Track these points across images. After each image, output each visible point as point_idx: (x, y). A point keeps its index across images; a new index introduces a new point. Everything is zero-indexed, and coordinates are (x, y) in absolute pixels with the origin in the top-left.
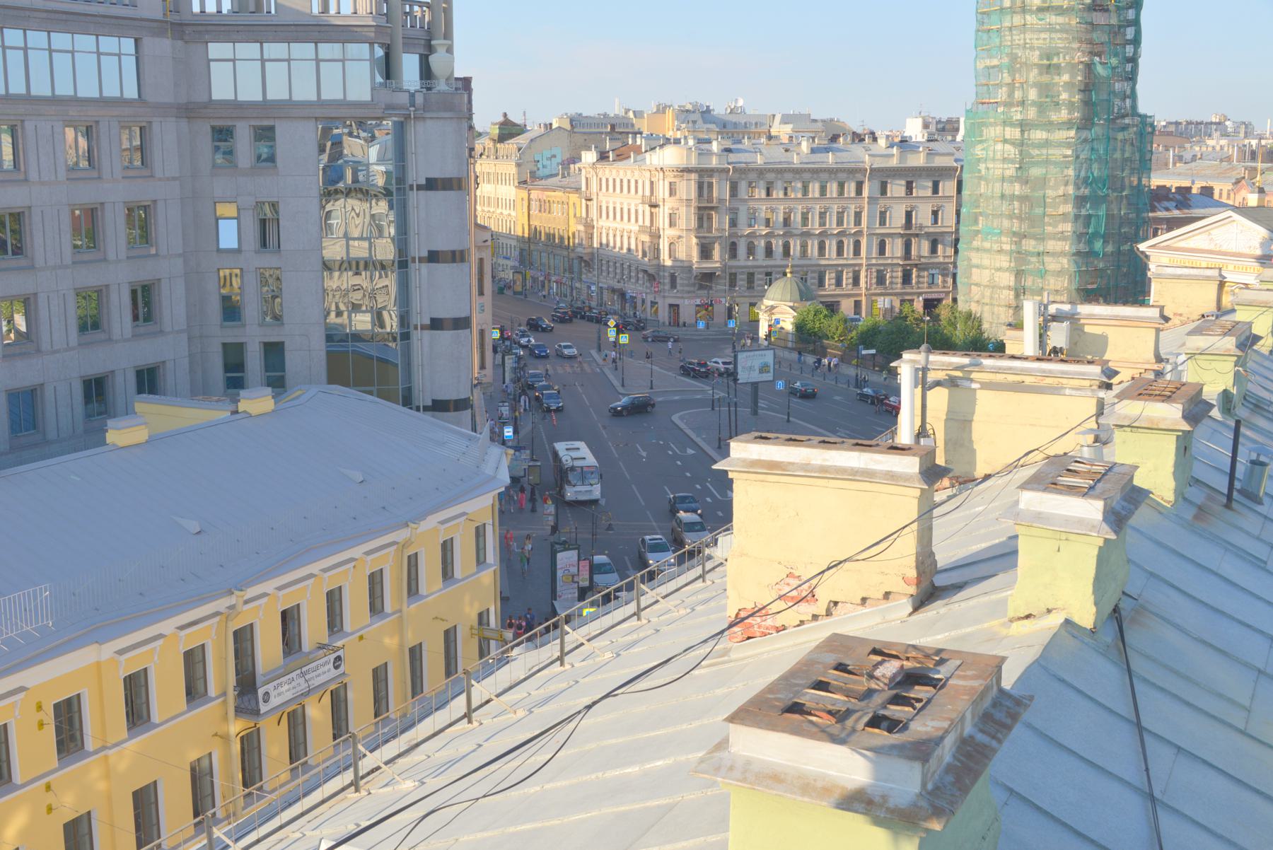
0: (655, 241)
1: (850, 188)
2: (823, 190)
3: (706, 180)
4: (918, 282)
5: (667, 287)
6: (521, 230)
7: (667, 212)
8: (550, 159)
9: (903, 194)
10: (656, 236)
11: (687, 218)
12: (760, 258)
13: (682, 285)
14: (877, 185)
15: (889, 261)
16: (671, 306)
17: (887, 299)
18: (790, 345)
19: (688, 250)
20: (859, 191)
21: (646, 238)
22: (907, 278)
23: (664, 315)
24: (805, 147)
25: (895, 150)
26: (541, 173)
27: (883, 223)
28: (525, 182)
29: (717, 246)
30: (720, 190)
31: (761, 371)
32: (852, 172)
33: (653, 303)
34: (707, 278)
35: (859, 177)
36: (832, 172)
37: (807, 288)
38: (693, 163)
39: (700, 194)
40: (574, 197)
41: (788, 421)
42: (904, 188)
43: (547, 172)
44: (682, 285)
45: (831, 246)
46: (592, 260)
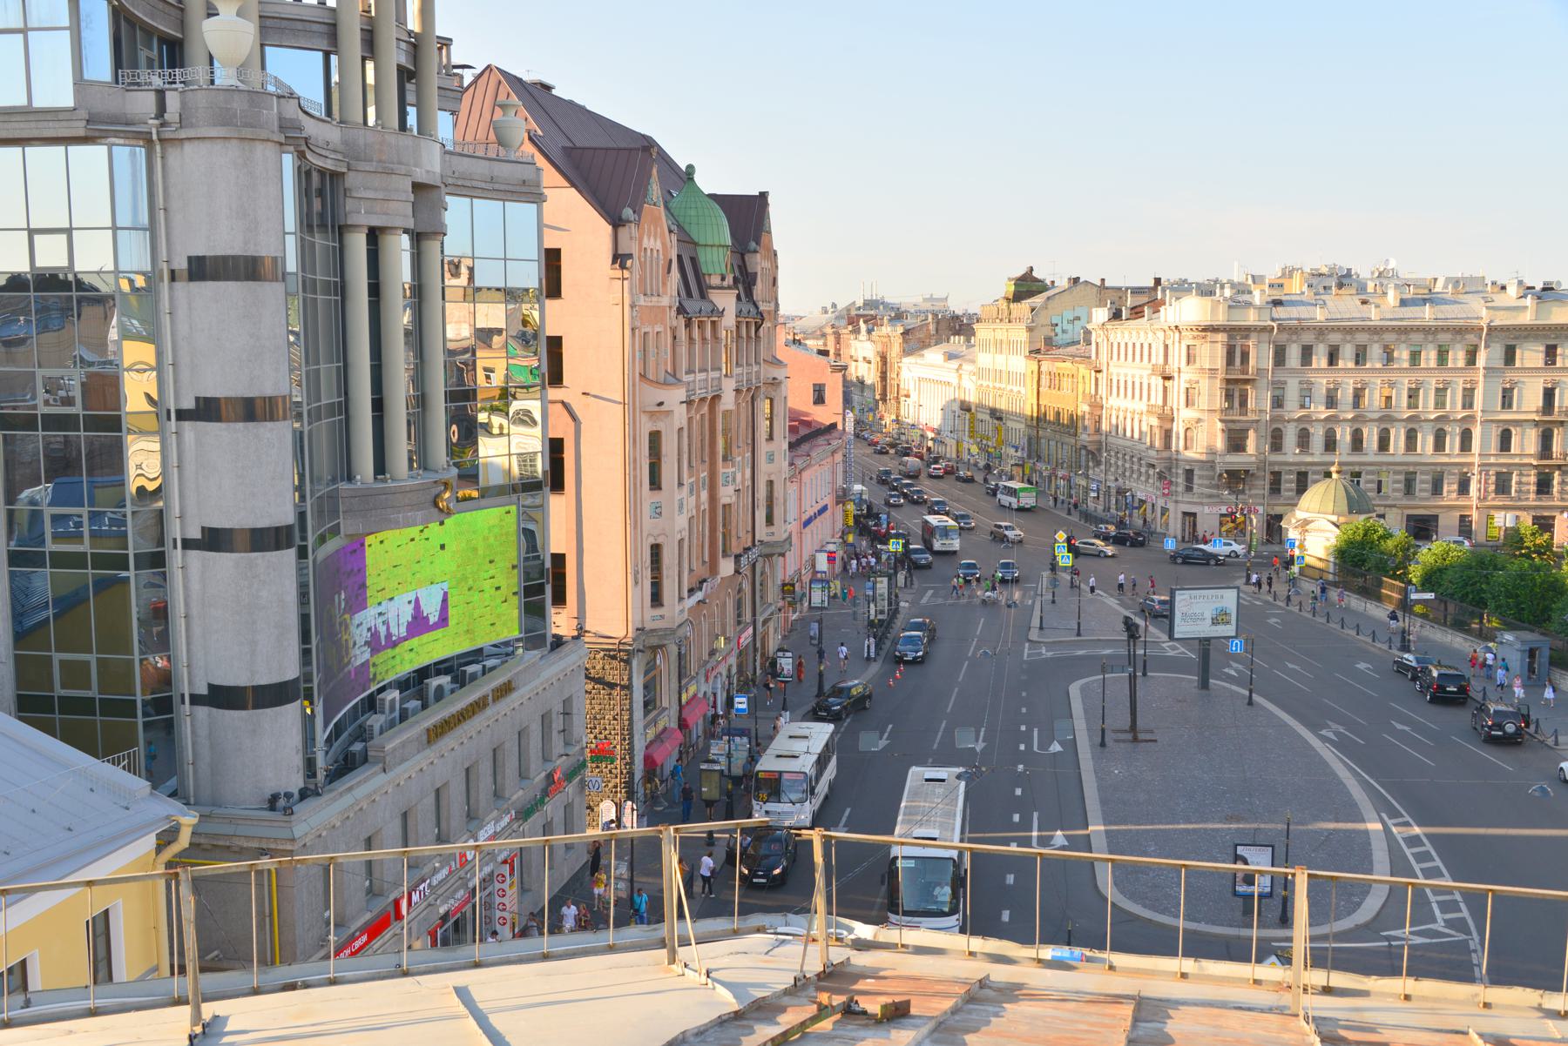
0: (1167, 426)
1: (1458, 357)
2: (1415, 357)
3: (1239, 342)
5: (1181, 489)
6: (1029, 408)
7: (1184, 386)
8: (1072, 322)
9: (1541, 364)
10: (1167, 418)
11: (1211, 394)
12: (1317, 452)
14: (1498, 351)
15: (1517, 460)
16: (1185, 514)
18: (1331, 577)
19: (1201, 434)
20: (1471, 359)
21: (1155, 422)
22: (1544, 486)
23: (1175, 524)
24: (1392, 298)
25: (1529, 301)
26: (1061, 338)
27: (1507, 401)
28: (1038, 351)
29: (1251, 434)
30: (1260, 356)
31: (1215, 622)
32: (1460, 331)
33: (1164, 511)
34: (1235, 479)
35: (1471, 338)
36: (1427, 331)
37: (1362, 494)
38: (1221, 319)
39: (1230, 360)
40: (1083, 370)
41: (1250, 703)
42: (1542, 356)
43: (1067, 338)
45: (1426, 442)
46: (1099, 450)
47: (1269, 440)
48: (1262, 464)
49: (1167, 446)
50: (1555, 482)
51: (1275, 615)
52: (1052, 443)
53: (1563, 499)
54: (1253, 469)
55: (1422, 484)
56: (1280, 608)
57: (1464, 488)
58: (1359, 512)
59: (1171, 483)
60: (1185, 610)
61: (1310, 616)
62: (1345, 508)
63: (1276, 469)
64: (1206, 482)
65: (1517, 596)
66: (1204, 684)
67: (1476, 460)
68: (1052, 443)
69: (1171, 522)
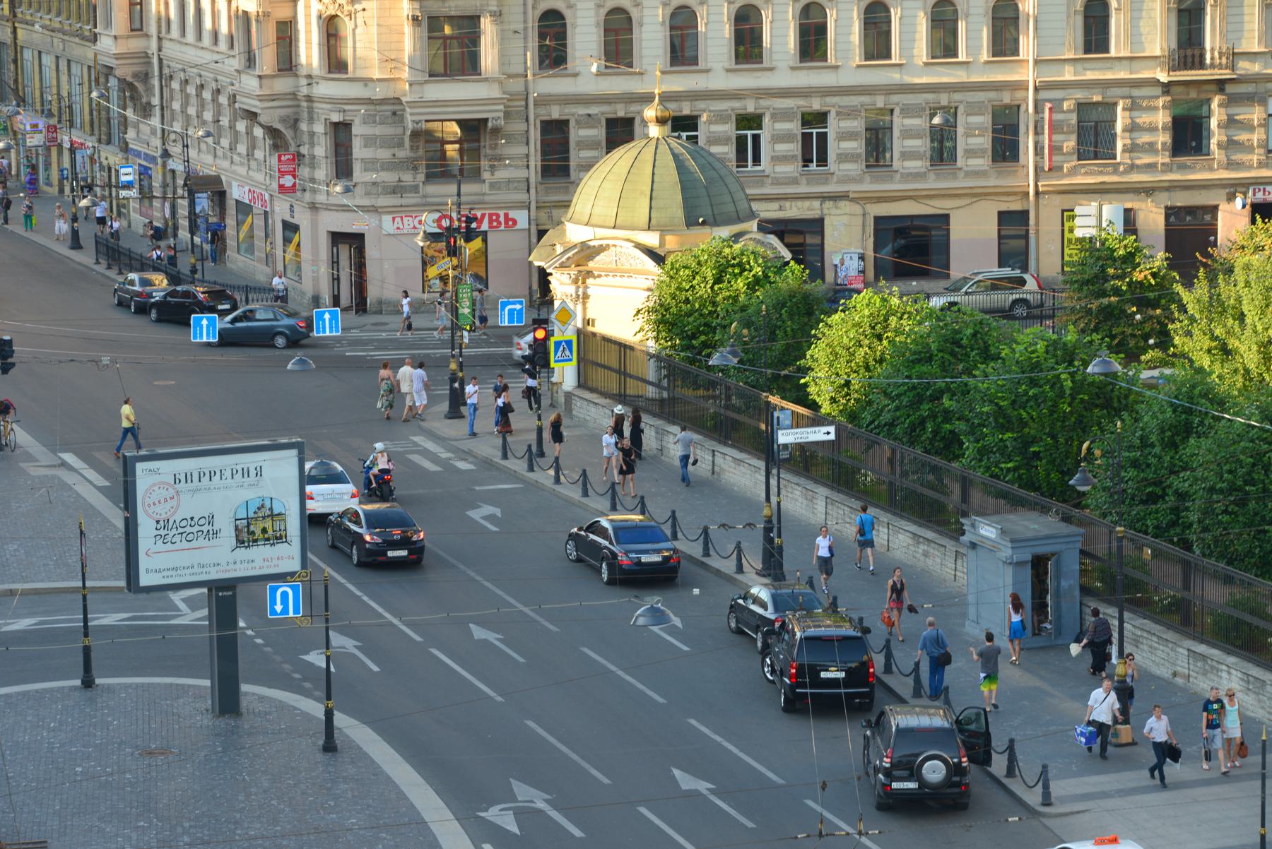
4: (1230, 145)
5: (321, 173)
13: (370, 165)
16: (337, 238)
17: (1111, 211)
18: (651, 392)
22: (1188, 135)
23: (316, 268)
29: (486, 24)
31: (246, 536)
33: (290, 228)
41: (330, 746)
44: (370, 165)
46: (145, 77)
47: (533, 42)
48: (517, 105)
49: (287, 64)
50: (1214, 123)
51: (491, 498)
52: (48, 60)
53: (1231, 165)
54: (494, 115)
55: (908, 142)
56: (513, 476)
57: (1005, 147)
58: (714, 221)
59: (298, 157)
60: (162, 511)
61: (575, 494)
62: (679, 213)
63: (555, 113)
64: (384, 154)
65: (1023, 424)
66: (228, 701)
67: (1029, 75)
68: (48, 60)
69: (306, 254)
